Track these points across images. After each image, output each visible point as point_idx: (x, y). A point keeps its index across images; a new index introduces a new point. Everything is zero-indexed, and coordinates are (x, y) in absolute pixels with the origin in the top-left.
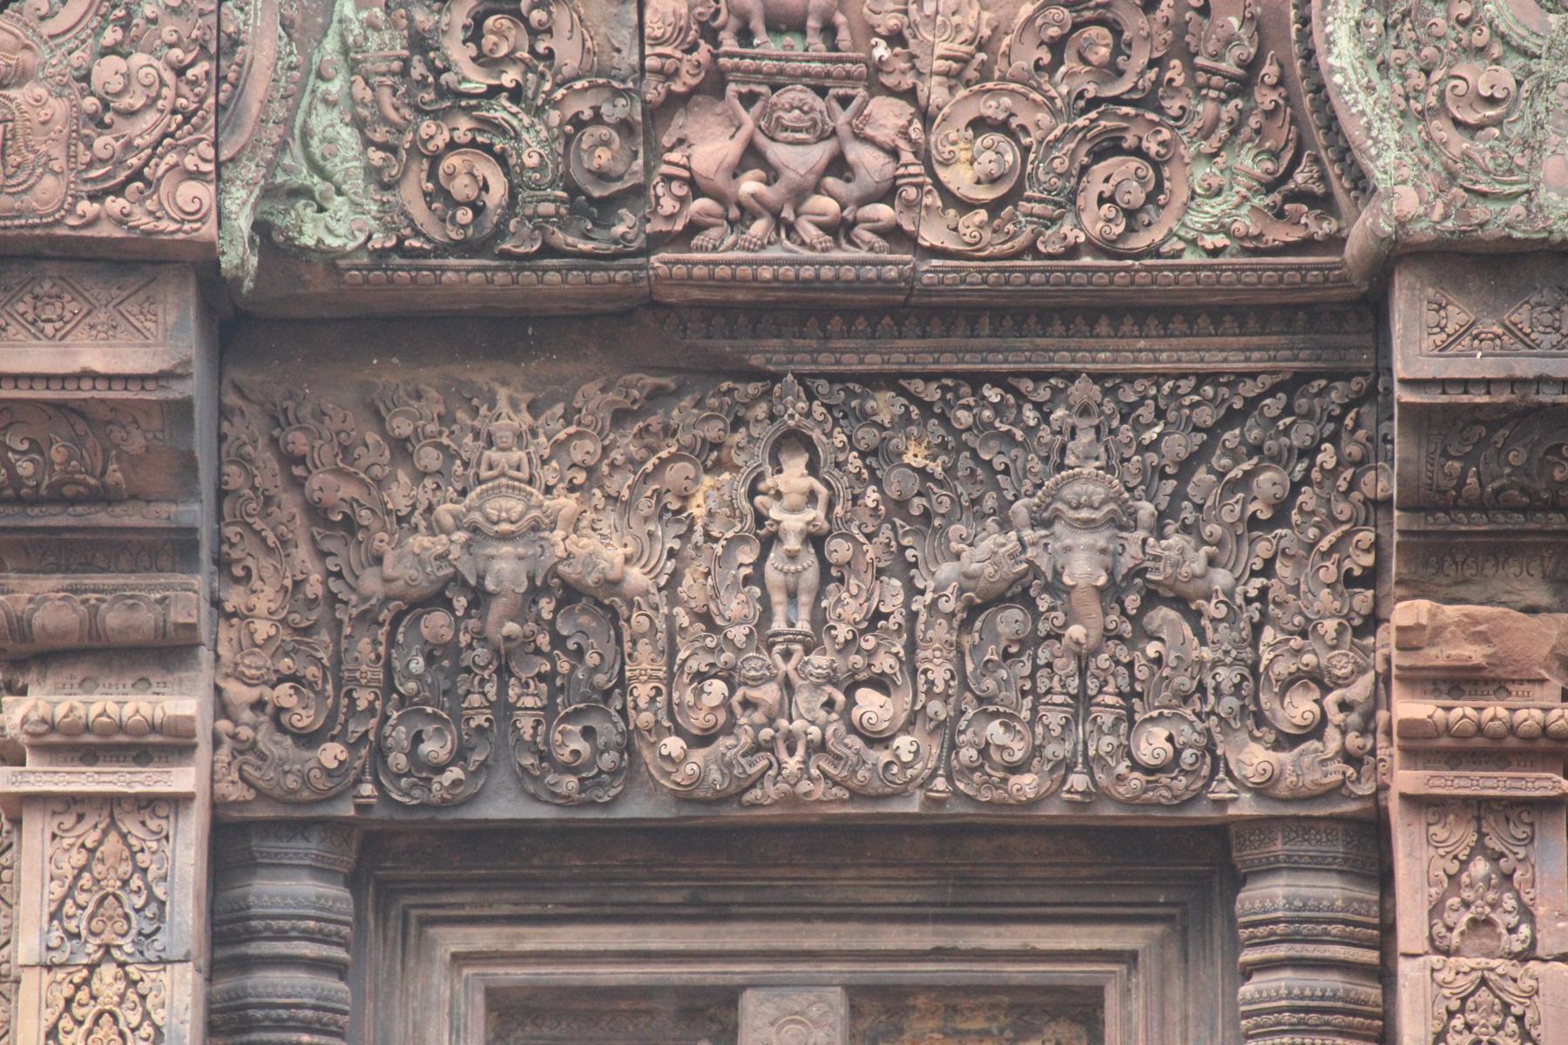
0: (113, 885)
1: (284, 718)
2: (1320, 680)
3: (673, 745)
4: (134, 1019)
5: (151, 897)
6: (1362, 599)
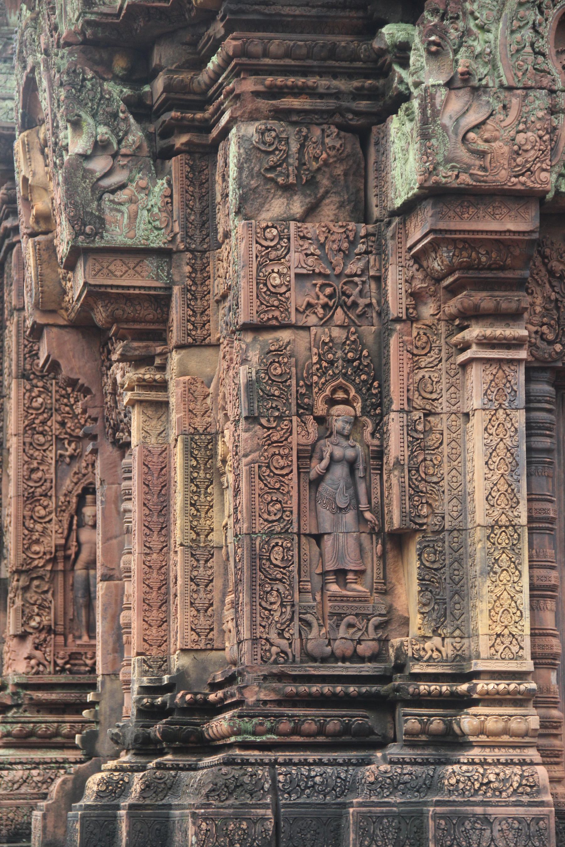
0: (501, 386)
1: (544, 336)
4: (509, 426)
5: (513, 390)
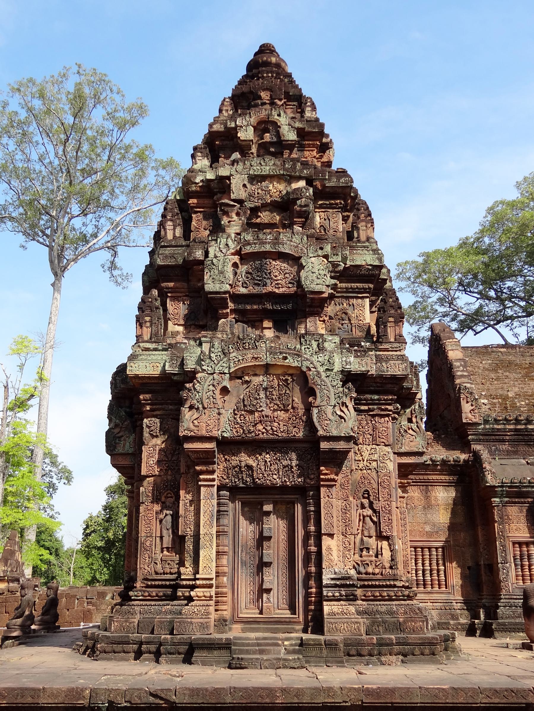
2: (314, 474)
3: (257, 480)
6: (317, 467)
